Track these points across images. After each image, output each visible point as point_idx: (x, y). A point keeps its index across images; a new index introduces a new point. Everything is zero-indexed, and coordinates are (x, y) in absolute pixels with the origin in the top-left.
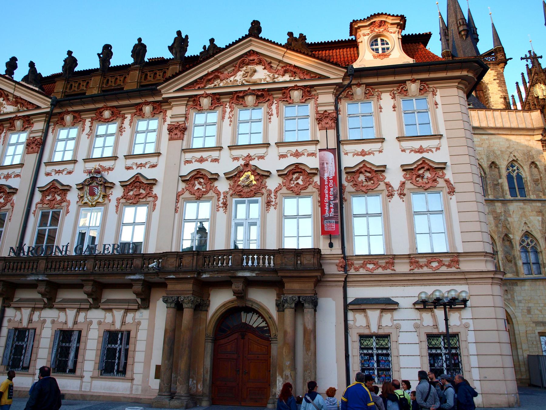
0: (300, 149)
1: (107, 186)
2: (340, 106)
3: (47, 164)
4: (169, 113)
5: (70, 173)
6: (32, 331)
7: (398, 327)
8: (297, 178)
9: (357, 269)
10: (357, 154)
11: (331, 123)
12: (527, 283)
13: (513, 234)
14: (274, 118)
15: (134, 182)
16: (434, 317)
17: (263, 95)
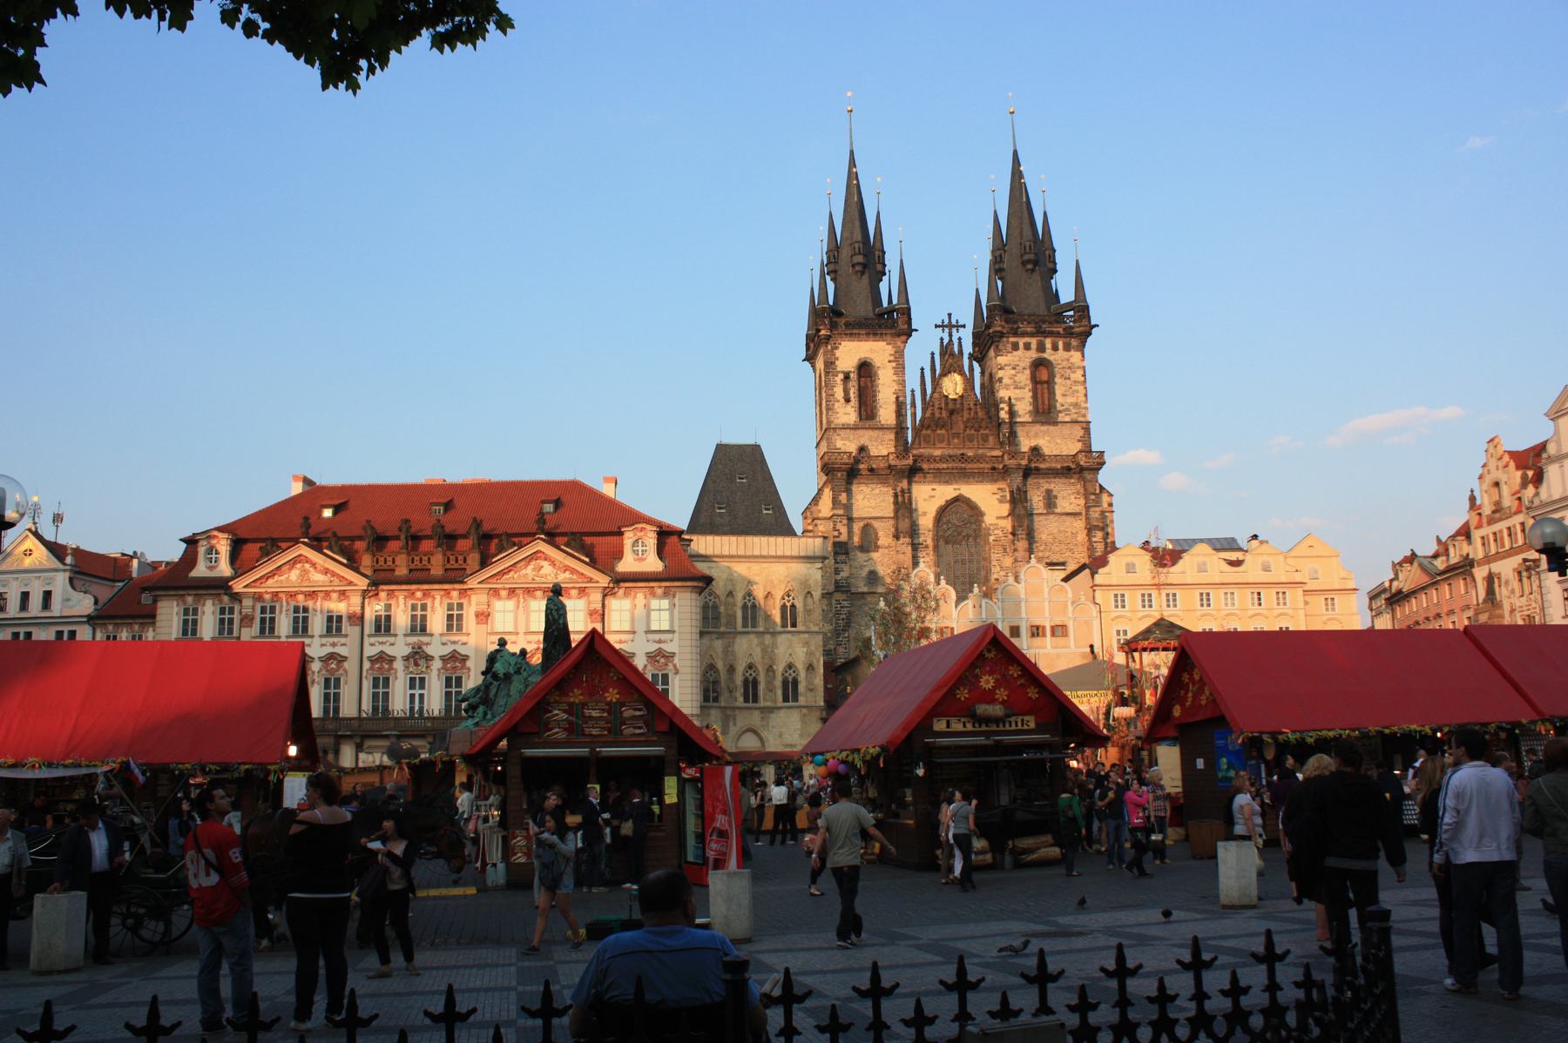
1: (429, 658)
4: (474, 598)
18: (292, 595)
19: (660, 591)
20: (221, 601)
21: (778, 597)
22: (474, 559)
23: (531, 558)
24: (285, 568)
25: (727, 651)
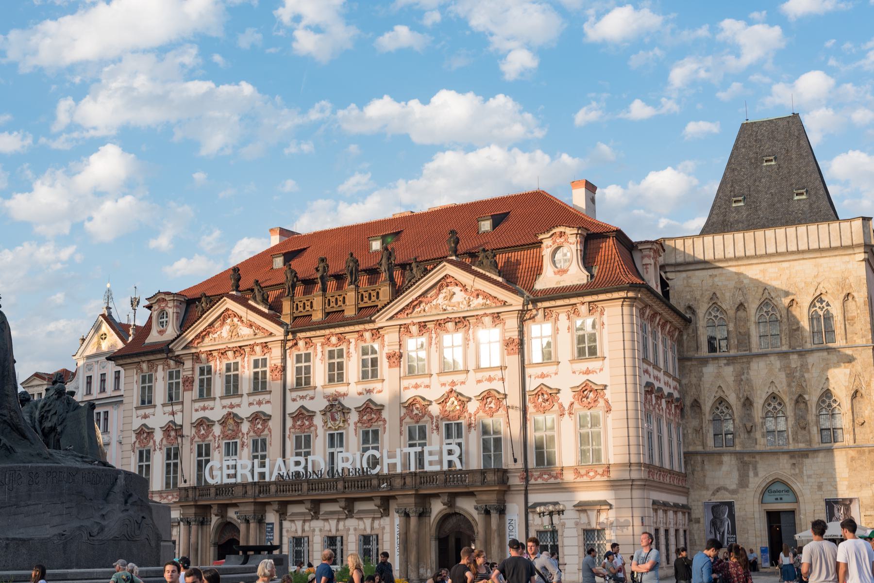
0: (492, 374)
1: (345, 411)
2: (525, 329)
3: (292, 390)
5: (312, 398)
6: (306, 539)
7: (563, 525)
8: (491, 402)
9: (536, 480)
10: (538, 377)
11: (516, 349)
12: (821, 455)
13: (809, 394)
14: (471, 343)
15: (367, 408)
16: (588, 516)
17: (461, 322)
18: (223, 353)
19: (583, 309)
20: (168, 365)
21: (806, 305)
22: (385, 291)
23: (440, 285)
24: (217, 324)
25: (740, 380)
